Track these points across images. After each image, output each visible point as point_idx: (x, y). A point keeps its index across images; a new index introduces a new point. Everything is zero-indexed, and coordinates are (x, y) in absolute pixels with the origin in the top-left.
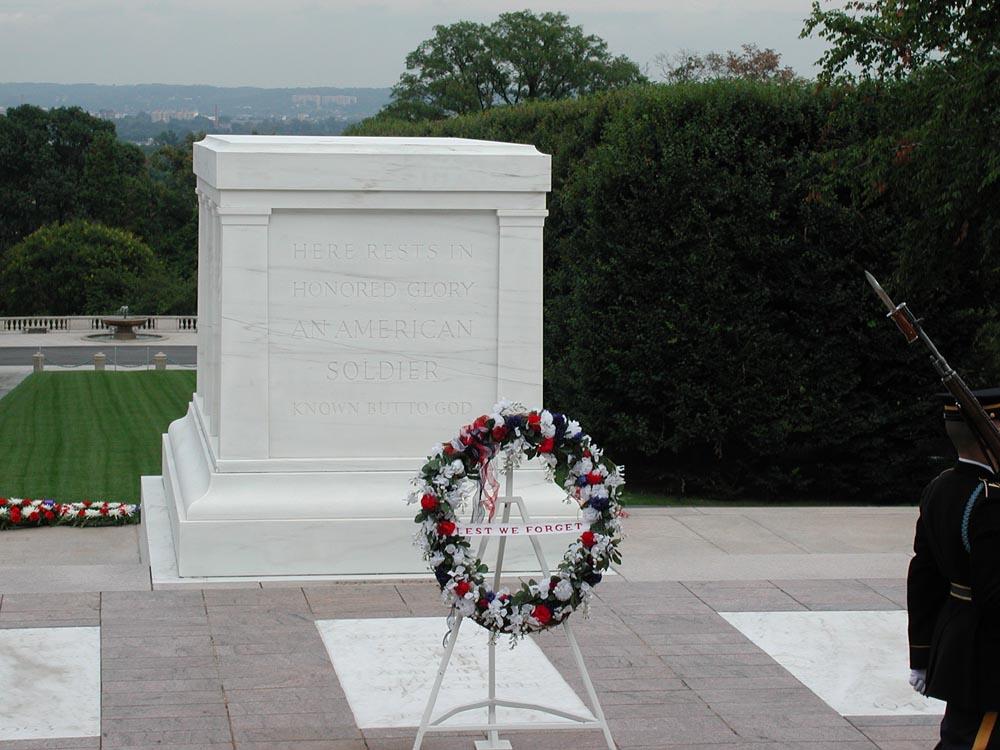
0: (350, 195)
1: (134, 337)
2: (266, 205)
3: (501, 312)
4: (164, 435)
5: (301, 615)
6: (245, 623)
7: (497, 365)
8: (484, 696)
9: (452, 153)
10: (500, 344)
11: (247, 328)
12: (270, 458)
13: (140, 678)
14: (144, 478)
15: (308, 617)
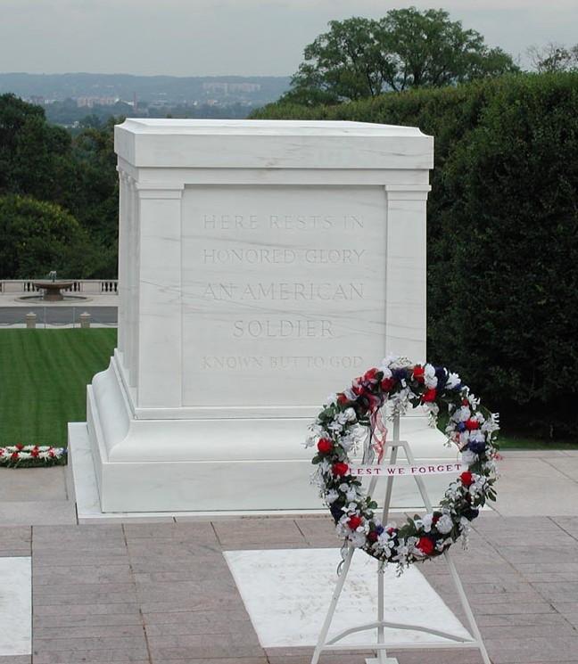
0: (255, 172)
1: (61, 298)
2: (179, 181)
3: (388, 277)
4: (88, 386)
5: (211, 547)
6: (160, 553)
7: (385, 324)
8: (374, 618)
9: (345, 134)
10: (388, 305)
11: (162, 291)
12: (183, 406)
13: (67, 603)
14: (70, 425)
15: (217, 549)
